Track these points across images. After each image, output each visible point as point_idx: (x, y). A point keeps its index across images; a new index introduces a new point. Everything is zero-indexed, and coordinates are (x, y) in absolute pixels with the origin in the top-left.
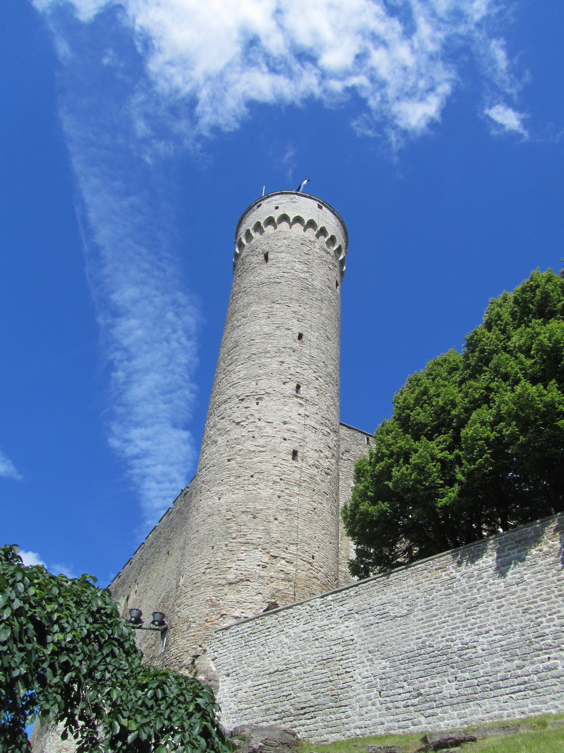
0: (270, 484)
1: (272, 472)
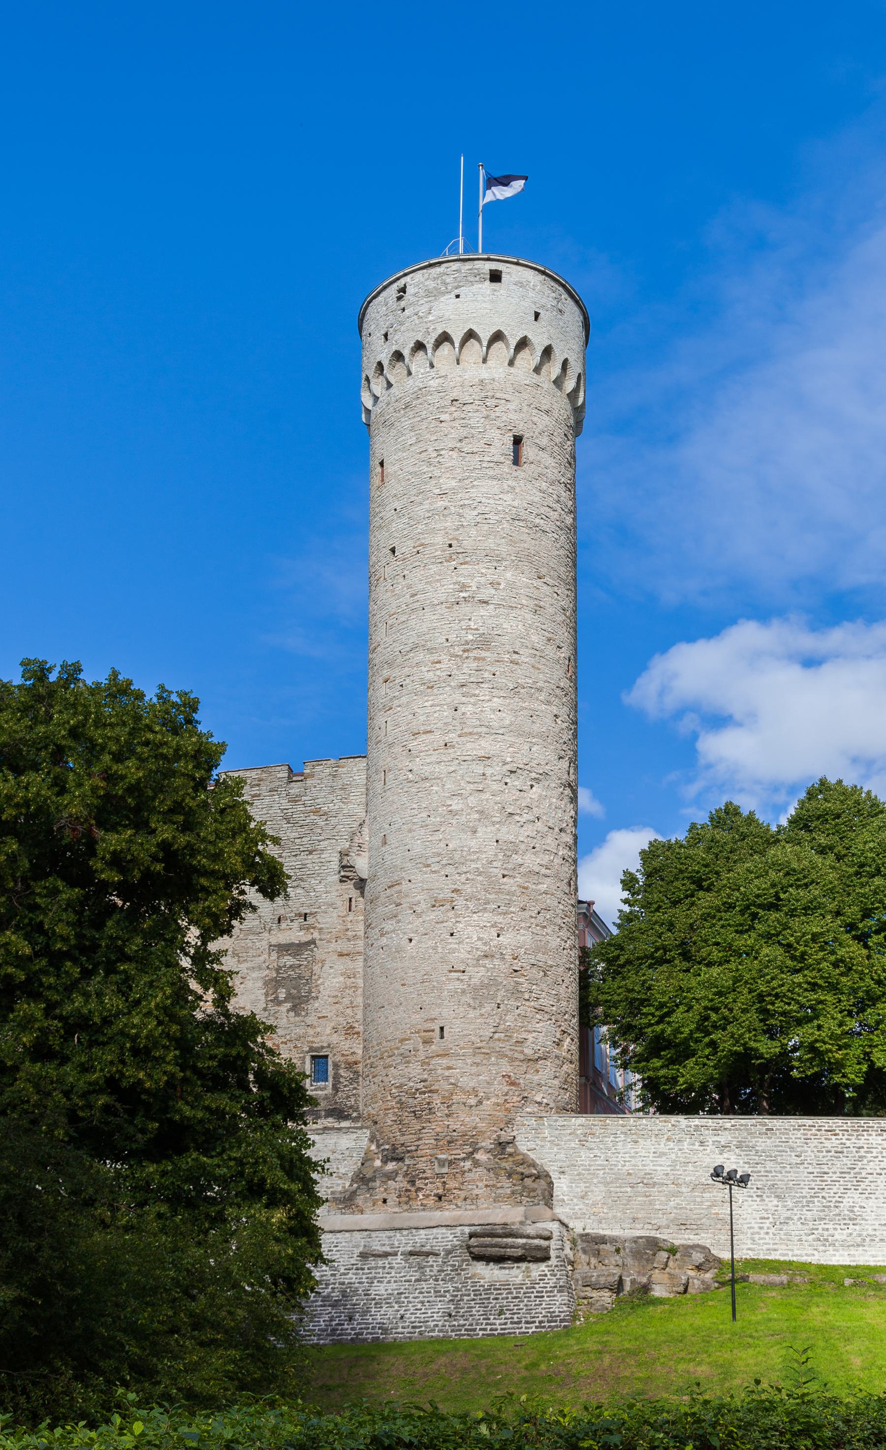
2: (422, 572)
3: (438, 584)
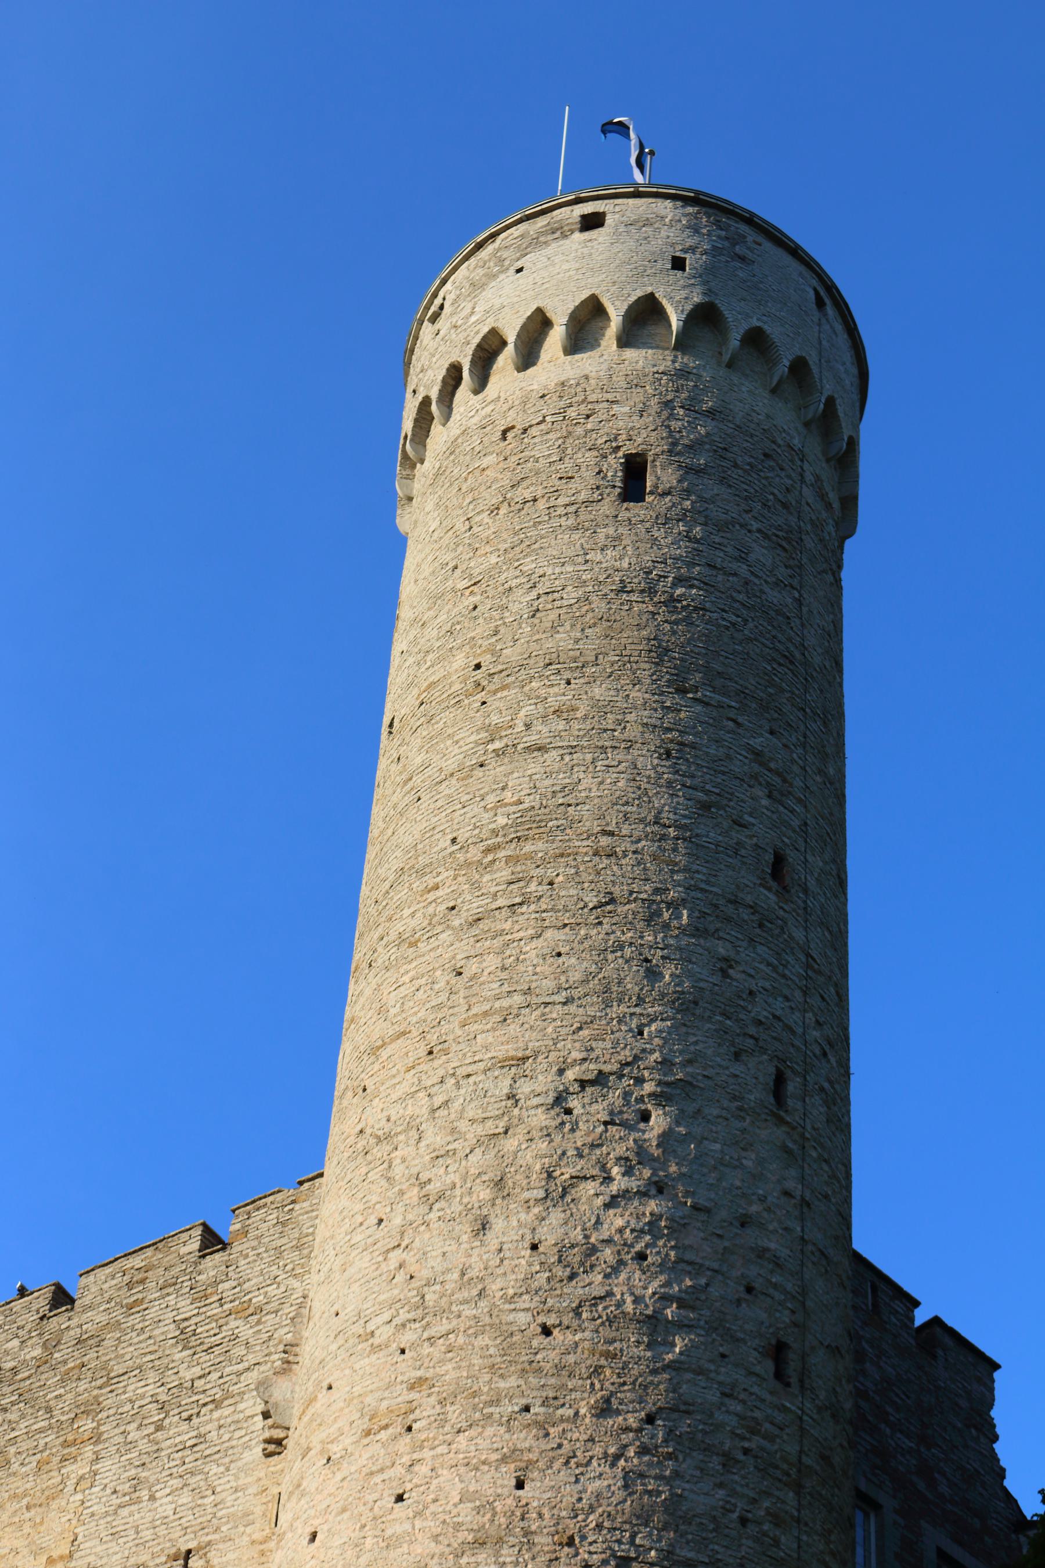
0: (715, 1463)
1: (719, 1416)
2: (425, 733)
3: (449, 742)
